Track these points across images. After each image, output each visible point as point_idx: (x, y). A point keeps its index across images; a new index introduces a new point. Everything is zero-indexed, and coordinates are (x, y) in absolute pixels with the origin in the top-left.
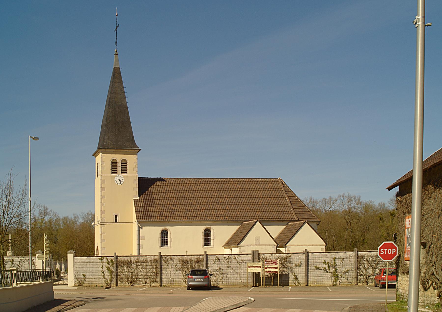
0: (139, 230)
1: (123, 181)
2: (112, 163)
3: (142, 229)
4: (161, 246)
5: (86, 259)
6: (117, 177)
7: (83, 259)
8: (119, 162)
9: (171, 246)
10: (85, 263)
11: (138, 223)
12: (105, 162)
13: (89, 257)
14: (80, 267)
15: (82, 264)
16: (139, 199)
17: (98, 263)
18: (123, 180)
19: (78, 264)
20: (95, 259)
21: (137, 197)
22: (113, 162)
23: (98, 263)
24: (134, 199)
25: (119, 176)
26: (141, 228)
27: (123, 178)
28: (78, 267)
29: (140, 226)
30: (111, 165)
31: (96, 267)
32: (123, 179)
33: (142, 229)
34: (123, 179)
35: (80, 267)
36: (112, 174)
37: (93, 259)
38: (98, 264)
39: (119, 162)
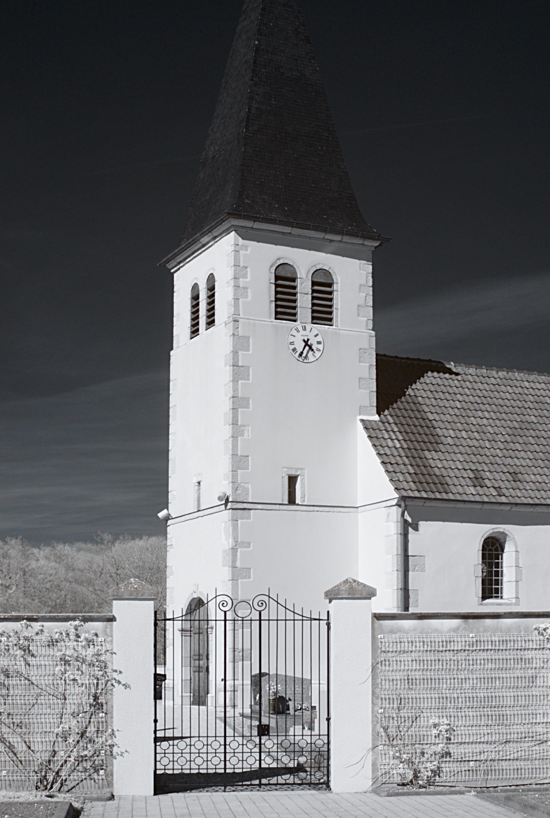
0: (405, 536)
1: (319, 350)
2: (277, 278)
3: (416, 529)
4: (484, 598)
5: (456, 630)
6: (298, 331)
7: (436, 630)
8: (304, 276)
9: (517, 598)
10: (449, 655)
11: (406, 508)
12: (248, 269)
13: (471, 621)
14: (417, 675)
15: (431, 657)
16: (381, 421)
17: (529, 655)
18: (321, 347)
19: (404, 657)
20: (509, 630)
21: (373, 415)
22: (283, 274)
23: (529, 655)
24: (362, 421)
25: (305, 329)
26: (410, 525)
27: (319, 338)
28: (398, 676)
29: (409, 520)
30: (273, 286)
31: (518, 673)
32: (319, 343)
33: (416, 529)
34: (319, 343)
35: (413, 675)
36: (276, 319)
37: (495, 630)
38: (530, 661)
39: (304, 276)
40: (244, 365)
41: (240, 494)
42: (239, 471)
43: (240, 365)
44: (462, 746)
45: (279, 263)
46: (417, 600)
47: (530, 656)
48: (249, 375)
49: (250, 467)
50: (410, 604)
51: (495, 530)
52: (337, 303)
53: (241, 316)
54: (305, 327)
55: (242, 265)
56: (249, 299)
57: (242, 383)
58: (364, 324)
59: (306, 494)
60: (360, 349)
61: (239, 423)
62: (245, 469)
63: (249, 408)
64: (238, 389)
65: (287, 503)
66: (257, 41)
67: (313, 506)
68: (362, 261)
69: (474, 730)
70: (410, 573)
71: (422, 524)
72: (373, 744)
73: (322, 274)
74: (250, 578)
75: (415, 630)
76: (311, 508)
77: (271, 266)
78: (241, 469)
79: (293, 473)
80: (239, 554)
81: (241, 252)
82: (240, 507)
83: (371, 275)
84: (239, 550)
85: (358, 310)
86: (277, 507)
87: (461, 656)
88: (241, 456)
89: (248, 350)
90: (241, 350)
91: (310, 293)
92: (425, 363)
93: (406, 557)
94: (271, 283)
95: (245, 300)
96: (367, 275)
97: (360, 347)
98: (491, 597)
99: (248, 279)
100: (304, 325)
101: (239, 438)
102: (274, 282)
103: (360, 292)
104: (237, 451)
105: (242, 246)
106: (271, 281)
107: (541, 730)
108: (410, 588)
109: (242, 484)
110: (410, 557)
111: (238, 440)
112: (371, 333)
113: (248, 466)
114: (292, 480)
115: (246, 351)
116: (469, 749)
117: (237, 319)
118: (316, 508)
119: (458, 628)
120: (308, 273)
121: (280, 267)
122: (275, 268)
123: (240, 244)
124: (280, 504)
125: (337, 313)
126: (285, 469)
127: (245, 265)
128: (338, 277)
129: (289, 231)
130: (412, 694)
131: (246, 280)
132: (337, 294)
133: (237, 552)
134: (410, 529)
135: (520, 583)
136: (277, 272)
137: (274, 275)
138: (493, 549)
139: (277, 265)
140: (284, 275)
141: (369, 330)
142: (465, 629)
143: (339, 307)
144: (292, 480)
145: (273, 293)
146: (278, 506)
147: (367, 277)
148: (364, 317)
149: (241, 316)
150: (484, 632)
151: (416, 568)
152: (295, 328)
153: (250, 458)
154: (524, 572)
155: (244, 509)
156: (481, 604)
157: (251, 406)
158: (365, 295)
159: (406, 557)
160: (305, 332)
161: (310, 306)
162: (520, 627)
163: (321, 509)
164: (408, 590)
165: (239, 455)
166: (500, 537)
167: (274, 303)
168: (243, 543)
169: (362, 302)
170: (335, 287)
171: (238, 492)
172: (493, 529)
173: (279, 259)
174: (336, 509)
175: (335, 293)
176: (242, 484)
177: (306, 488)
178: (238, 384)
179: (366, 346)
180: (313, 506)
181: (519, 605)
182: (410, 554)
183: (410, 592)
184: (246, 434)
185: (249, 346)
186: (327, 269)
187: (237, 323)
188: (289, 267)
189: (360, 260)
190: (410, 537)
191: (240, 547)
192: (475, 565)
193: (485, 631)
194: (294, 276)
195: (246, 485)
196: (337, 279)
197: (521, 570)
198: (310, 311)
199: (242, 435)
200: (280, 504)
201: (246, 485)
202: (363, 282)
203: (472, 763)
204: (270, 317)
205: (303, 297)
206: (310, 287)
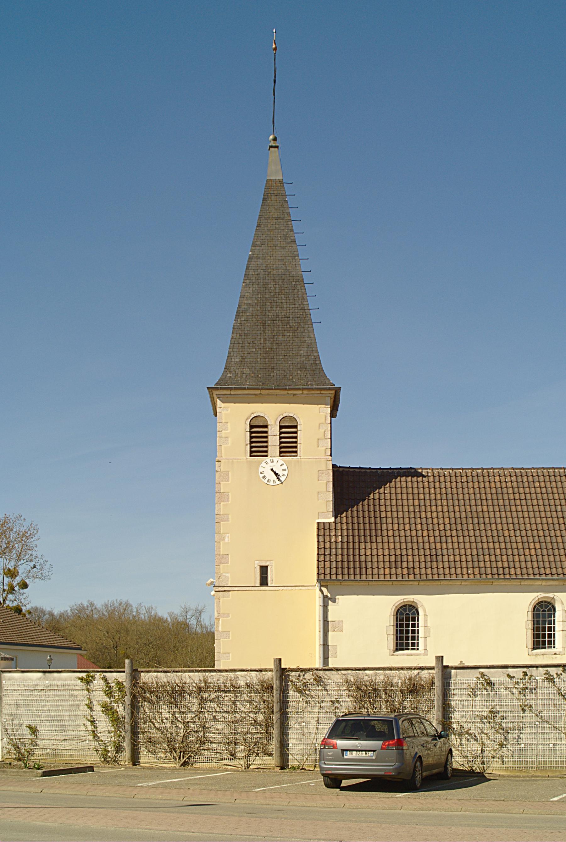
0: (325, 607)
1: (284, 475)
2: (252, 427)
3: (334, 601)
4: (397, 650)
5: (40, 679)
6: (267, 463)
7: (30, 679)
8: (273, 423)
9: (425, 650)
10: (36, 693)
11: (321, 586)
12: (229, 424)
13: (47, 674)
14: (21, 702)
15: (28, 693)
16: (335, 522)
17: (76, 693)
18: (286, 473)
19: (15, 693)
20: (66, 680)
21: (330, 518)
22: (255, 423)
23: (76, 693)
24: (318, 523)
25: (272, 461)
26: (330, 599)
27: (285, 467)
28: (13, 702)
29: (329, 595)
30: (249, 433)
31: (71, 703)
32: (284, 470)
33: (334, 601)
34: (284, 470)
35: (19, 702)
36: (251, 456)
37: (59, 679)
38: (76, 696)
39: (273, 423)
40: (224, 491)
41: (222, 581)
42: (221, 565)
43: (222, 492)
44: (43, 741)
45: (253, 416)
46: (336, 652)
47: (76, 694)
48: (228, 499)
49: (229, 562)
50: (330, 656)
51: (405, 600)
52: (301, 439)
53: (224, 457)
54: (273, 460)
55: (223, 422)
56: (229, 445)
57: (223, 505)
58: (323, 452)
59: (274, 578)
60: (318, 471)
61: (221, 532)
62: (226, 563)
63: (229, 521)
64: (220, 509)
65: (259, 585)
66: (251, 251)
67: (279, 586)
68: (319, 406)
69: (50, 732)
70: (330, 634)
71: (341, 599)
72: (2, 737)
73: (288, 419)
74: (229, 637)
75: (20, 678)
76: (278, 588)
77: (247, 419)
78: (223, 564)
79: (264, 564)
80: (220, 622)
81: (223, 412)
82: (221, 590)
83: (329, 415)
84: (221, 619)
85: (318, 442)
86: (250, 588)
87: (42, 693)
88: (223, 555)
89: (228, 481)
90: (222, 481)
91: (278, 434)
92: (404, 470)
93: (326, 622)
94: (246, 431)
95: (226, 446)
96: (325, 416)
97: (319, 470)
98: (402, 650)
99: (229, 431)
100: (272, 458)
101: (221, 543)
102: (249, 430)
103: (319, 428)
104: (220, 552)
105: (224, 408)
106: (247, 430)
107: (82, 734)
108: (329, 644)
109: (223, 574)
110: (329, 622)
111: (220, 544)
112: (328, 458)
113: (228, 561)
114: (264, 570)
115: (227, 481)
116: (48, 742)
117: (220, 460)
118: (280, 588)
119: (41, 678)
120: (276, 421)
121: (254, 419)
122: (250, 420)
123: (222, 407)
124: (252, 587)
125: (300, 446)
126: (257, 562)
127: (227, 421)
128: (301, 421)
129: (260, 393)
130: (19, 712)
131: (227, 432)
132: (301, 433)
133: (219, 620)
134: (330, 602)
135: (428, 638)
136: (251, 423)
137: (249, 425)
138: (410, 614)
139: (251, 418)
140: (257, 424)
141: (328, 456)
142: (44, 678)
143: (302, 442)
144: (264, 570)
145: (249, 438)
146: (251, 588)
147: (326, 417)
148: (322, 447)
149: (224, 457)
150: (53, 680)
151: (336, 630)
152: (265, 461)
153: (229, 556)
154: (431, 630)
155: (225, 591)
156: (393, 655)
157: (230, 520)
158: (323, 430)
159: (326, 622)
160: (273, 463)
161: (278, 444)
162: (71, 678)
163: (285, 588)
164: (328, 645)
165: (221, 554)
166: (413, 604)
167: (249, 445)
168: (224, 614)
169: (321, 436)
170: (299, 427)
171: (221, 580)
172: (403, 599)
173: (253, 414)
174: (297, 588)
175: (299, 432)
176: (223, 574)
177: (274, 574)
178: (220, 505)
179: (323, 468)
180: (279, 586)
181: (427, 655)
182: (329, 620)
183: (330, 647)
184: (226, 540)
185: (229, 478)
186: (292, 416)
187: (220, 463)
188: (262, 418)
189: (318, 405)
190: (330, 607)
191: (222, 617)
192: (387, 626)
193: (54, 680)
194: (265, 424)
195: (227, 575)
196: (300, 422)
197: (430, 629)
198: (278, 447)
199: (224, 540)
200: (252, 587)
201: (227, 575)
202: (323, 420)
203: (48, 750)
204: (246, 456)
205: (272, 438)
206: (278, 430)
